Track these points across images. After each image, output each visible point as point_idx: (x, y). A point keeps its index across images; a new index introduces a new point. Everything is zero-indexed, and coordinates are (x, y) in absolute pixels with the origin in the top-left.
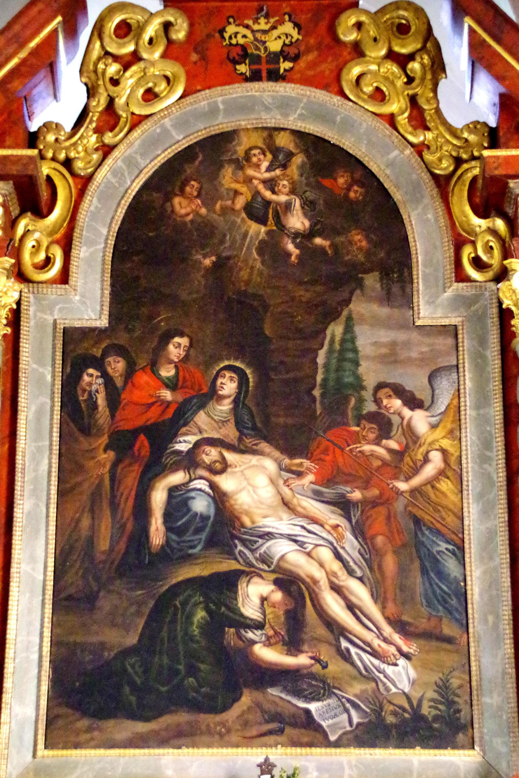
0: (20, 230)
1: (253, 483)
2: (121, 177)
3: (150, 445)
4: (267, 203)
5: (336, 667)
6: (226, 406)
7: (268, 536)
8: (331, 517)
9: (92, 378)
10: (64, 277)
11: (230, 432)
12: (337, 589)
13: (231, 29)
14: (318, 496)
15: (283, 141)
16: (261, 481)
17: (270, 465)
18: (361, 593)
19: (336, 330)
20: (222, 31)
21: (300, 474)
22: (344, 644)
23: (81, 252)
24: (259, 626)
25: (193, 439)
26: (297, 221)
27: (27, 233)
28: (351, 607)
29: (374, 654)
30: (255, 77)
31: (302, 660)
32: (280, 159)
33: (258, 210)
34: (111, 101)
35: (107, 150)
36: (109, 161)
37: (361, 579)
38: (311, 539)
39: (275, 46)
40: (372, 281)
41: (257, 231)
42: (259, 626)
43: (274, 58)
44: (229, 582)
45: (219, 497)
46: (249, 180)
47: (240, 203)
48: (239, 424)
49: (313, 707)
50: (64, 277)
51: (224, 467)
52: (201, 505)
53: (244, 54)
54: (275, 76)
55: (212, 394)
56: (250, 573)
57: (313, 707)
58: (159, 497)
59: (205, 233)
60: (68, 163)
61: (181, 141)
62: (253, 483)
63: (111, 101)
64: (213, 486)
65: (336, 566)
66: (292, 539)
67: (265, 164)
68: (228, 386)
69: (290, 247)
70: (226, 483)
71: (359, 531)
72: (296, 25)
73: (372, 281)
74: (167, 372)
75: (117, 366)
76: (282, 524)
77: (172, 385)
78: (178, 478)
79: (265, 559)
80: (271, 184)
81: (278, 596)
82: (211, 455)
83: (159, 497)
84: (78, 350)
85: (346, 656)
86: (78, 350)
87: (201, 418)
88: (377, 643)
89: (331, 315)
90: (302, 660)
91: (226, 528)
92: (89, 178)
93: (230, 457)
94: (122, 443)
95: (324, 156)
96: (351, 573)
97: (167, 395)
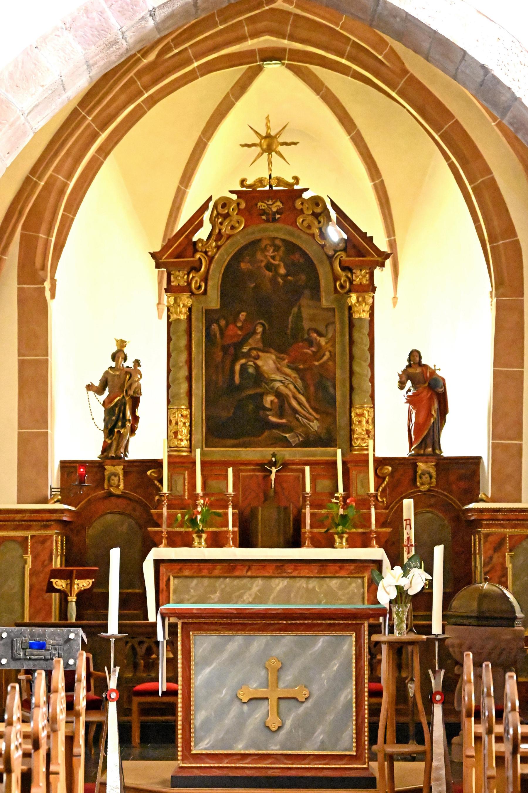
0: (191, 276)
1: (268, 363)
2: (223, 257)
3: (234, 351)
4: (272, 264)
5: (294, 423)
6: (259, 336)
7: (273, 380)
8: (294, 374)
9: (215, 327)
10: (205, 292)
11: (260, 345)
12: (296, 398)
13: (260, 204)
14: (289, 367)
15: (278, 242)
16: (271, 362)
17: (274, 357)
18: (303, 399)
19: (295, 310)
20: (257, 205)
21: (284, 360)
22: (297, 416)
23: (210, 283)
24: (270, 410)
25: (248, 348)
26: (282, 271)
27: (193, 277)
28: (300, 404)
29: (307, 418)
30: (267, 221)
31: (284, 421)
32: (277, 248)
33: (269, 267)
34: (220, 230)
35: (218, 247)
36: (220, 251)
37: (302, 395)
38: (286, 381)
39: (274, 209)
40: (307, 292)
41: (268, 274)
42: (270, 410)
43: (274, 214)
44: (261, 396)
45: (257, 367)
46: (266, 256)
47: (263, 264)
48: (263, 343)
49: (287, 435)
50: (205, 292)
51: (258, 357)
52: (251, 370)
53: (264, 212)
54: (274, 220)
55: (254, 332)
56: (268, 393)
57: (287, 435)
58: (237, 368)
59: (251, 274)
60: (206, 253)
61: (243, 242)
62: (268, 363)
63: (220, 230)
64: (255, 364)
65: (294, 390)
66: (281, 381)
67: (271, 251)
68: (260, 329)
69: (280, 280)
70: (259, 363)
71: (302, 379)
72: (281, 202)
73: (307, 292)
74: (239, 324)
75: (223, 322)
76: (278, 377)
77: (241, 328)
78: (243, 361)
79: (272, 388)
80: (273, 258)
81: (276, 400)
82: (254, 353)
83: (237, 368)
84: (210, 316)
85: (297, 419)
86: (210, 316)
87: (251, 341)
88: (307, 415)
89: (292, 305)
90: (284, 421)
91: (259, 378)
92: (213, 257)
93: (260, 354)
94: (225, 349)
95: (291, 248)
96: (300, 393)
97: (239, 332)
